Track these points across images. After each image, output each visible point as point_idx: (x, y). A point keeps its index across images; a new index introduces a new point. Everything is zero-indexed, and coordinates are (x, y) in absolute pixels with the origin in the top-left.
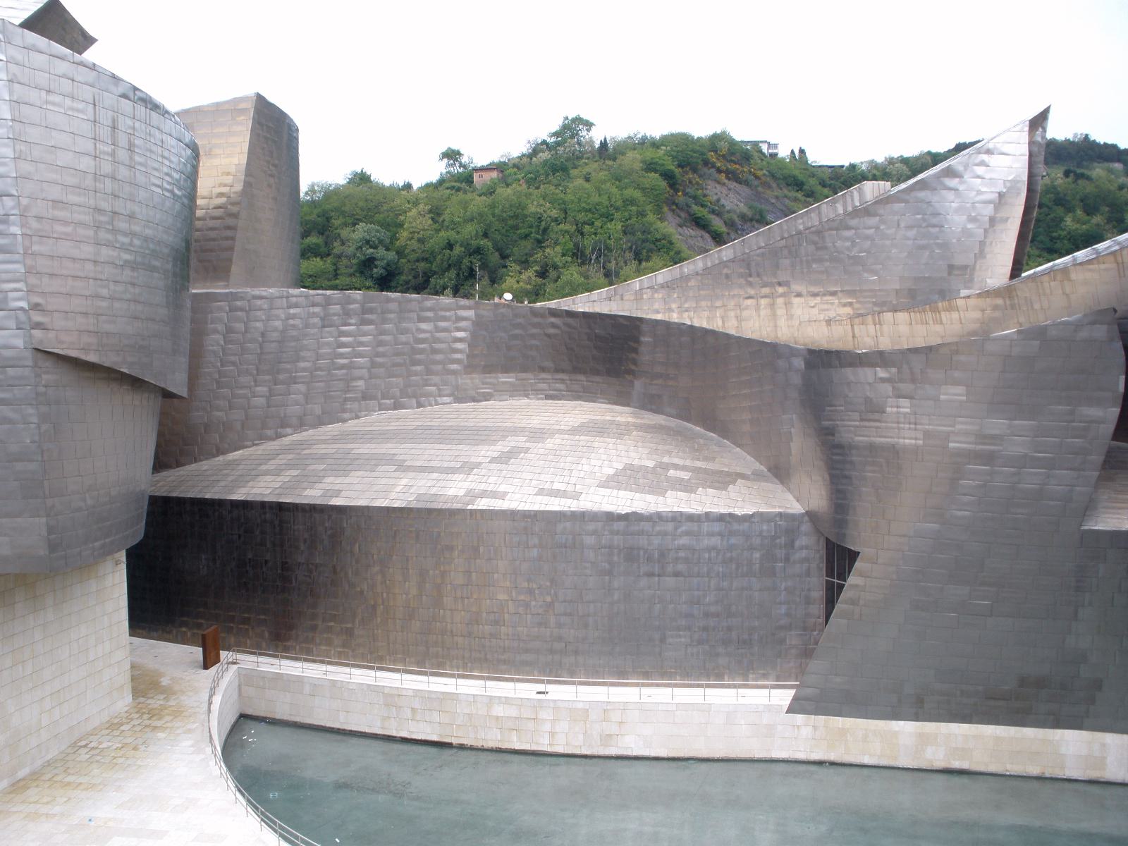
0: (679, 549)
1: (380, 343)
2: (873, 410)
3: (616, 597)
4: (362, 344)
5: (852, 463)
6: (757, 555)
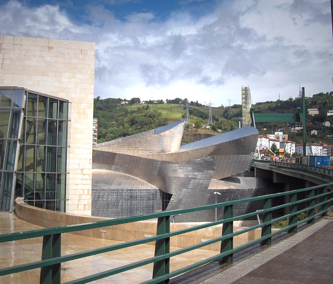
0: (139, 195)
2: (175, 171)
3: (128, 205)
5: (171, 180)
6: (151, 196)
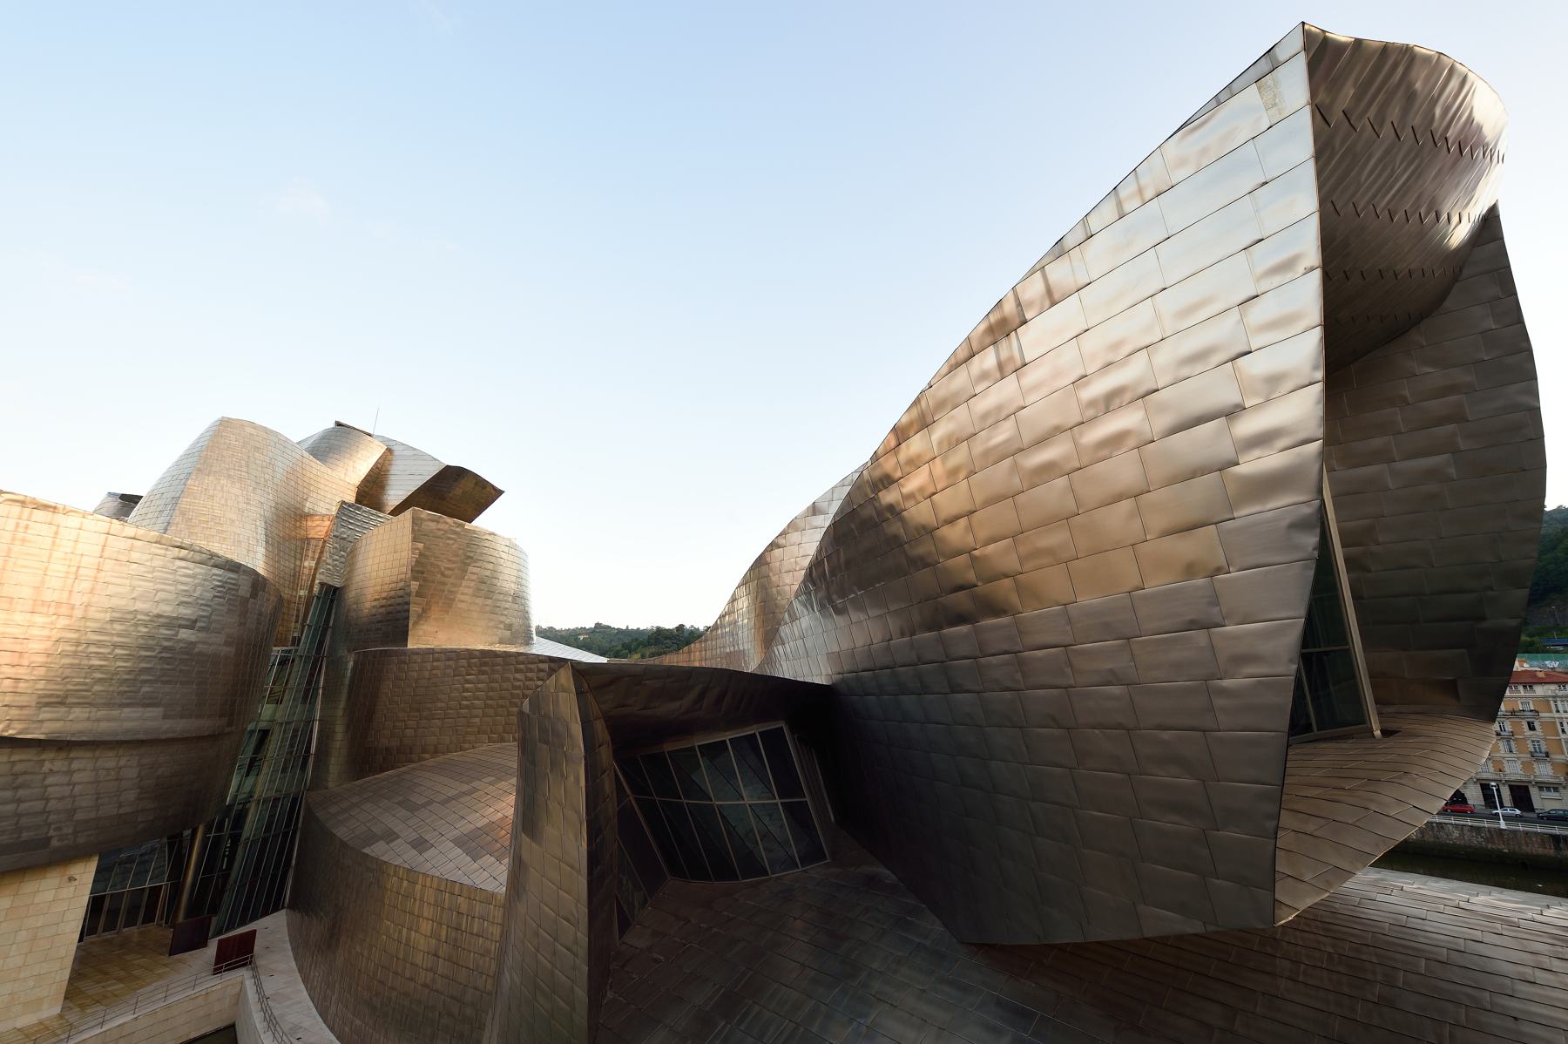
1: (492, 689)
4: (479, 690)
